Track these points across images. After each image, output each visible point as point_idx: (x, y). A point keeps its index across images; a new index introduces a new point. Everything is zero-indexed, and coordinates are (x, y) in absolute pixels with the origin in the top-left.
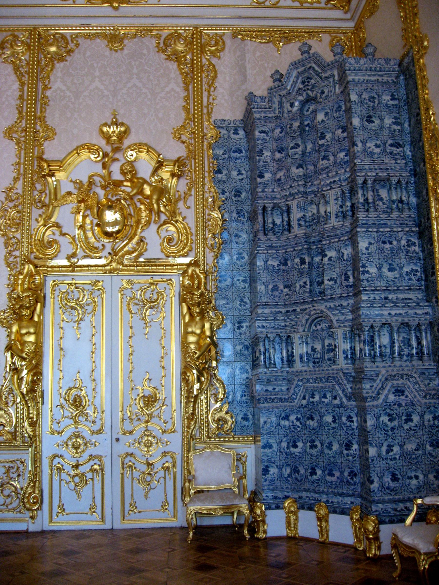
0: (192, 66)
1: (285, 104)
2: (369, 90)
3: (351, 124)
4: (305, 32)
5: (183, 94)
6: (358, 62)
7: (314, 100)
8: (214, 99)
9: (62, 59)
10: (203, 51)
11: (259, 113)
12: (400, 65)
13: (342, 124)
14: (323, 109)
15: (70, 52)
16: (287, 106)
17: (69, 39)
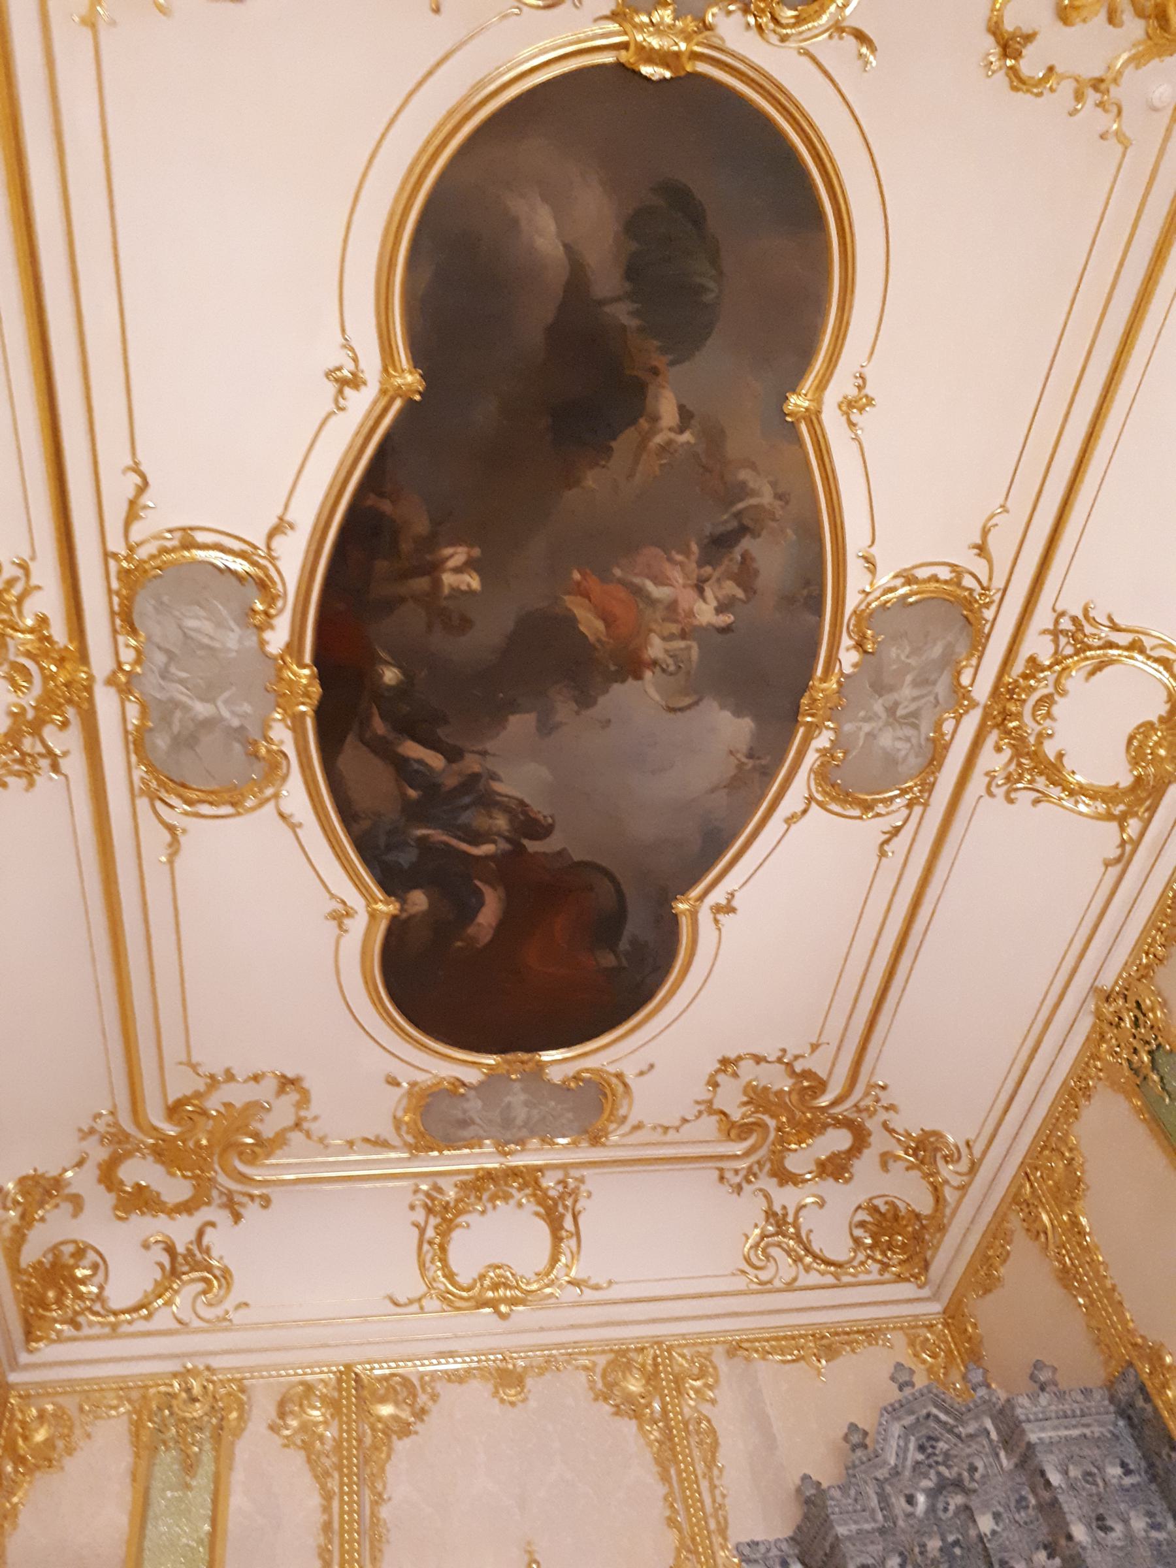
0: (668, 1427)
1: (893, 1500)
2: (1075, 1458)
3: (1070, 1537)
4: (858, 1332)
5: (662, 1490)
6: (1035, 1403)
7: (958, 1485)
8: (724, 1496)
9: (405, 1430)
10: (680, 1391)
11: (846, 1523)
12: (1112, 1399)
13: (1040, 1538)
14: (986, 1505)
15: (421, 1414)
16: (900, 1504)
17: (416, 1383)
